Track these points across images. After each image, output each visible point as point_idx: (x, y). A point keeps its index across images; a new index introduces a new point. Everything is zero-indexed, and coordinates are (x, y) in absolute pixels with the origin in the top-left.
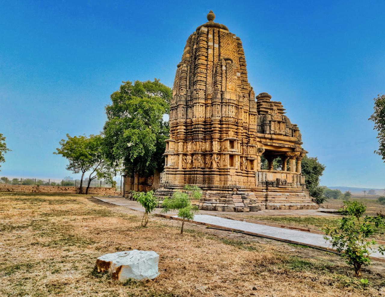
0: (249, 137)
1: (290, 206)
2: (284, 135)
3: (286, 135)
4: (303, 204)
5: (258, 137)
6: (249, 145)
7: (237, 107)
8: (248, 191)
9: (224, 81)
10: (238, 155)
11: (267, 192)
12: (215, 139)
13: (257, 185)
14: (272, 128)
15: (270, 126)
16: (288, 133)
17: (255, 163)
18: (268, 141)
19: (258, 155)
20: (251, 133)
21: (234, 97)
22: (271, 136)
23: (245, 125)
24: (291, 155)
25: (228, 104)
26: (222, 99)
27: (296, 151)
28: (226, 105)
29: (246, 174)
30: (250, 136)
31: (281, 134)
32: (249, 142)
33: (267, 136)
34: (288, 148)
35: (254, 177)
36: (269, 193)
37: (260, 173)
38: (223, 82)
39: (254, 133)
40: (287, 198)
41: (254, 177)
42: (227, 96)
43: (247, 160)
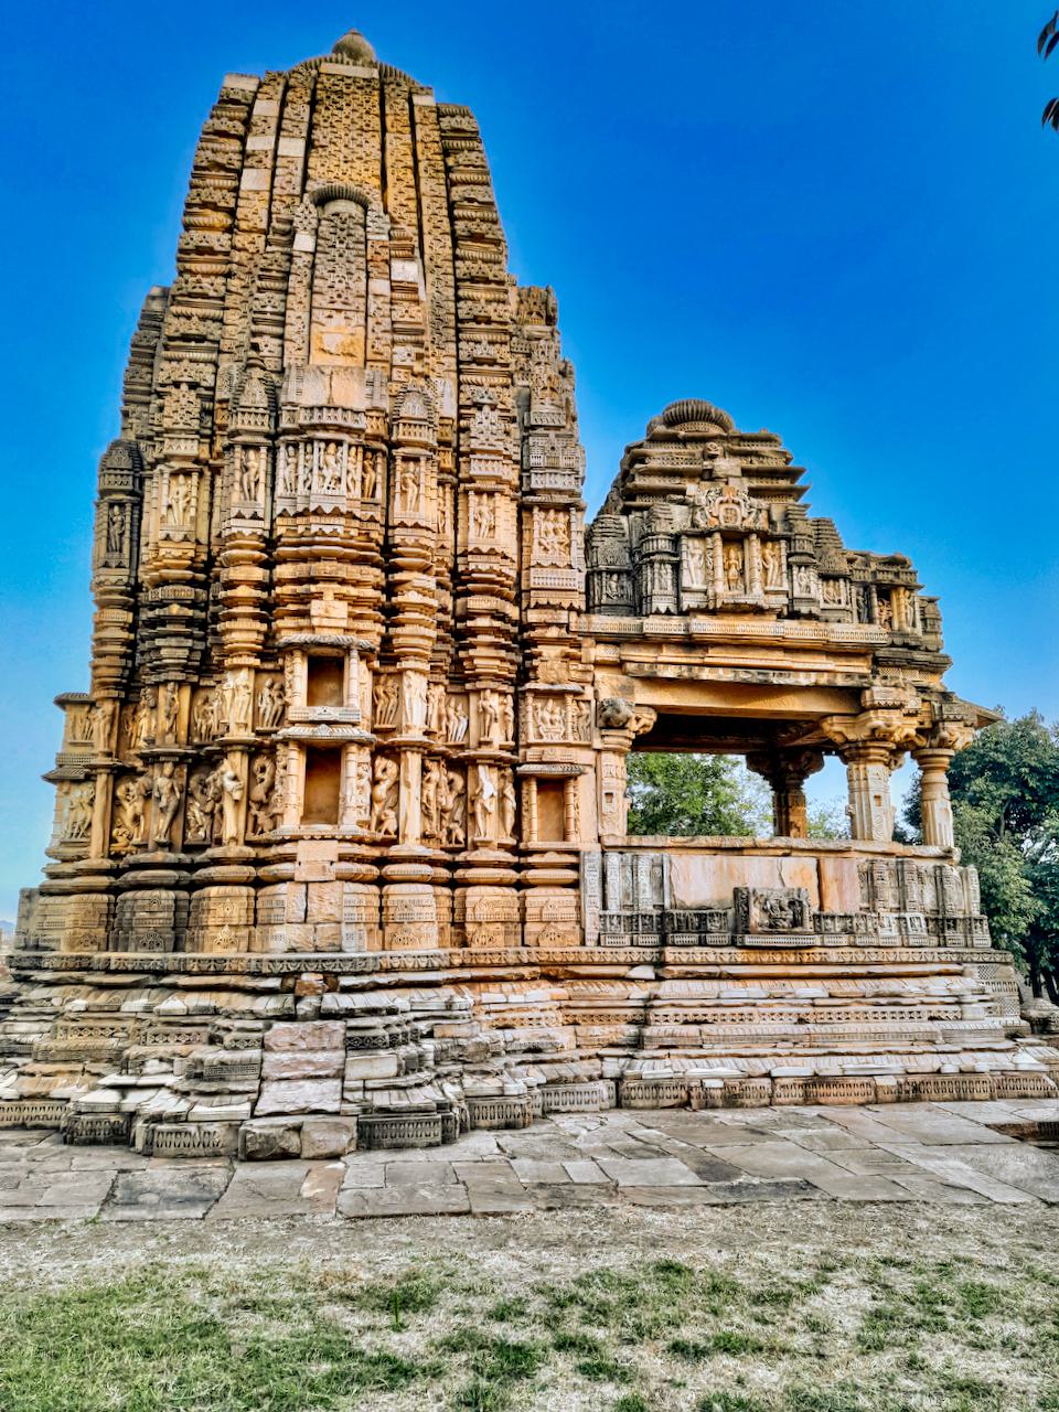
0: (534, 643)
1: (817, 1080)
2: (780, 616)
3: (794, 615)
4: (929, 1063)
5: (601, 639)
7: (383, 450)
8: (502, 979)
9: (296, 316)
10: (361, 744)
11: (659, 979)
12: (232, 653)
13: (591, 937)
14: (692, 577)
15: (677, 567)
16: (812, 601)
17: (581, 795)
18: (668, 654)
19: (597, 744)
21: (352, 394)
22: (687, 626)
23: (484, 567)
24: (851, 737)
25: (303, 437)
26: (275, 408)
27: (876, 708)
28: (296, 446)
29: (518, 867)
30: (537, 633)
31: (758, 611)
32: (524, 674)
33: (653, 625)
34: (816, 689)
35: (575, 885)
36: (667, 989)
37: (614, 859)
38: (291, 317)
39: (563, 617)
40: (801, 1021)
41: (575, 885)
42: (305, 393)
43: (519, 781)
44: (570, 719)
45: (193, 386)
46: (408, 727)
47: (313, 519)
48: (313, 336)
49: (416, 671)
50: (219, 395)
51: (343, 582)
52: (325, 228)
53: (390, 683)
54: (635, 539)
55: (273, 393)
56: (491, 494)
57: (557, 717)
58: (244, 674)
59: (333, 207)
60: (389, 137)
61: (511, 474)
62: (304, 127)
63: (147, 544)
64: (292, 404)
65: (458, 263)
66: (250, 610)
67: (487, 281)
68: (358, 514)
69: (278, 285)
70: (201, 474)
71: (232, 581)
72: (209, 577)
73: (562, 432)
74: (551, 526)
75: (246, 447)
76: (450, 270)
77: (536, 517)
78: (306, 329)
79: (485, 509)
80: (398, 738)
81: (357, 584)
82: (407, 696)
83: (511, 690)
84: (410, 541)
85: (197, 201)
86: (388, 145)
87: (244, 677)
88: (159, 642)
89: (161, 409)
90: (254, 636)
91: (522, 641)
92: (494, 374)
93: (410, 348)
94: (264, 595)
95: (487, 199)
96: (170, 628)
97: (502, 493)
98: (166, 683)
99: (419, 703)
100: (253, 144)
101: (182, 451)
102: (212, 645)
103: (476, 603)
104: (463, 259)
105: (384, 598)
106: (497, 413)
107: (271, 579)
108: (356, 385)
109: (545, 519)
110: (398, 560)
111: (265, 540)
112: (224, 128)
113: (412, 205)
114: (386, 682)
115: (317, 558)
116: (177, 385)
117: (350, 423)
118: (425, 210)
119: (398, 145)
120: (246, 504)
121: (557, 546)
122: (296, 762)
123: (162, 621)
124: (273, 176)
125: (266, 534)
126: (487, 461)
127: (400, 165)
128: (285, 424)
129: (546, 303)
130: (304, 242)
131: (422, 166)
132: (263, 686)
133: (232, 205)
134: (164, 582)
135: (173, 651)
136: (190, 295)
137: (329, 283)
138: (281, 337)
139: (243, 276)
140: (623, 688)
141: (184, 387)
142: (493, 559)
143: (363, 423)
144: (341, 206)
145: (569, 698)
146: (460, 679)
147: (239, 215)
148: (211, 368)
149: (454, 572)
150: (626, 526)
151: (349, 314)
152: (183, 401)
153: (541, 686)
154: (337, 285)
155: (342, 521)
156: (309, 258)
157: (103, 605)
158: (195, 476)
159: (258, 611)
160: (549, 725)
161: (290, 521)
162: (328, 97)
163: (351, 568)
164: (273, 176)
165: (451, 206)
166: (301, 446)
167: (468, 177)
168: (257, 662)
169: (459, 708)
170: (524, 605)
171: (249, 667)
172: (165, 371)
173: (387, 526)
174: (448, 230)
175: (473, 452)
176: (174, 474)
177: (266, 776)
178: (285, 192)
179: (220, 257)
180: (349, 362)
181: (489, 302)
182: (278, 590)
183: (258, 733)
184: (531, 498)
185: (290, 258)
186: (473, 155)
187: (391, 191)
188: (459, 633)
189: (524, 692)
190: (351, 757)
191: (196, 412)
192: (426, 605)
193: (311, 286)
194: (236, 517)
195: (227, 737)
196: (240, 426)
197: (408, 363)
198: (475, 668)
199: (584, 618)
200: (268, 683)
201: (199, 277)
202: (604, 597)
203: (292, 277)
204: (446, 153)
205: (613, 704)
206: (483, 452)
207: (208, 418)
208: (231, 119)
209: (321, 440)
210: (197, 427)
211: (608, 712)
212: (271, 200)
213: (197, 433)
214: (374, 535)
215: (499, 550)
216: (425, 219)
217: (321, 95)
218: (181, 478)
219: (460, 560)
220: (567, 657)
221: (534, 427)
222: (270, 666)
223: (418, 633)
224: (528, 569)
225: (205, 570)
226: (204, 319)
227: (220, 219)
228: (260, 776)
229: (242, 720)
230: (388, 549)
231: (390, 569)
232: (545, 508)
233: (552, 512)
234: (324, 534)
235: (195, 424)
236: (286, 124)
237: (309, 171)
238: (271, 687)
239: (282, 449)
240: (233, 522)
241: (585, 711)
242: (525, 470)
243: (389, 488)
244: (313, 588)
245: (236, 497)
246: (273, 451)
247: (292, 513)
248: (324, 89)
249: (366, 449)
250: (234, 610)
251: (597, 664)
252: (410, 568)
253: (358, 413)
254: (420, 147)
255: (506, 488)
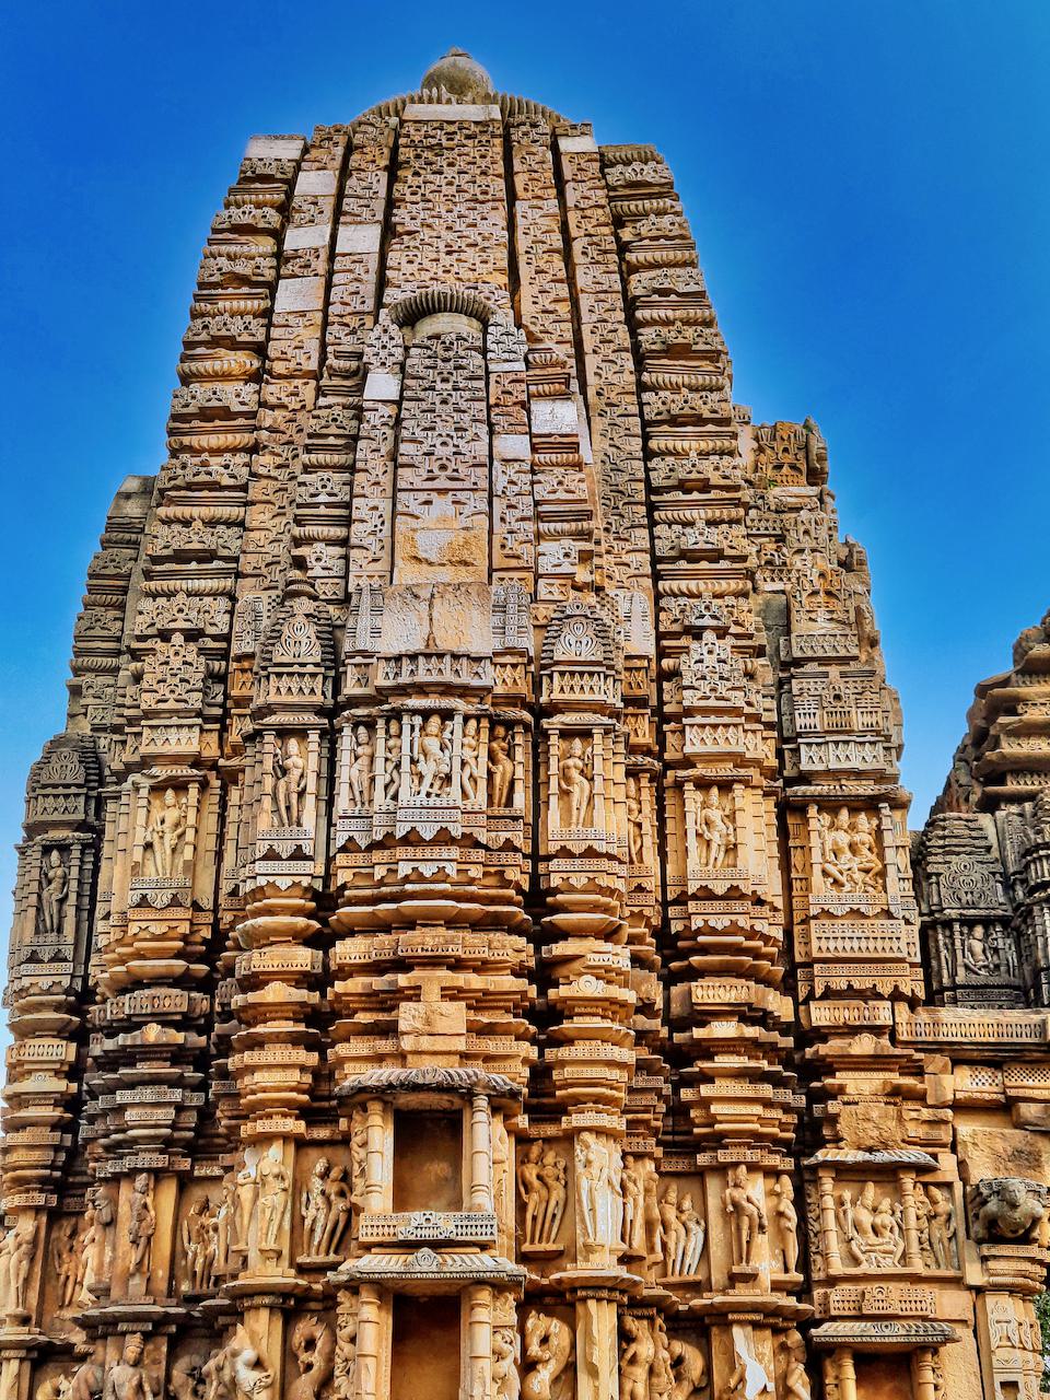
0: (826, 1067)
5: (960, 1056)
6: (826, 1154)
7: (525, 721)
9: (369, 506)
10: (499, 1287)
12: (256, 1110)
19: (975, 1275)
20: (846, 1013)
21: (471, 630)
25: (384, 709)
26: (334, 661)
28: (370, 725)
30: (832, 1047)
32: (812, 1132)
38: (361, 508)
39: (882, 1013)
42: (388, 632)
43: (818, 1358)
44: (913, 1223)
45: (192, 635)
46: (589, 1249)
47: (400, 852)
48: (398, 537)
49: (599, 1132)
50: (235, 650)
51: (457, 965)
52: (416, 360)
53: (550, 1158)
54: (1011, 857)
55: (331, 637)
56: (725, 786)
57: (886, 1219)
58: (275, 1151)
59: (428, 327)
60: (520, 207)
61: (761, 748)
62: (379, 206)
63: (107, 917)
64: (364, 653)
65: (646, 397)
66: (289, 1027)
67: (699, 420)
68: (483, 838)
69: (336, 459)
70: (204, 785)
71: (255, 975)
72: (214, 969)
73: (853, 667)
74: (843, 839)
75: (283, 733)
76: (635, 409)
77: (813, 824)
78: (388, 524)
79: (716, 815)
80: (570, 1272)
81: (483, 967)
82: (584, 1184)
83: (788, 1164)
84: (580, 881)
85: (204, 336)
86: (519, 221)
87: (275, 1157)
88: (122, 1097)
89: (137, 678)
90: (294, 1077)
91: (804, 1065)
92: (718, 576)
93: (567, 542)
94: (314, 998)
95: (693, 288)
96: (143, 1068)
97: (747, 783)
98: (132, 1174)
99: (608, 1200)
100: (295, 239)
101: (172, 748)
102: (218, 1096)
103: (707, 992)
104: (654, 388)
105: (533, 991)
106: (729, 641)
107: (326, 965)
108: (475, 613)
109: (832, 826)
110: (559, 918)
111: (315, 896)
112: (246, 220)
113: (564, 309)
114: (541, 1158)
115: (409, 923)
116: (165, 636)
117: (466, 679)
118: (585, 316)
119: (537, 218)
120: (284, 830)
121: (858, 876)
122: (372, 1326)
123: (128, 1056)
124: (329, 286)
125: (318, 885)
126: (715, 726)
127: (541, 248)
128: (351, 688)
129: (806, 448)
130: (382, 385)
131: (577, 247)
132: (310, 1171)
133: (261, 338)
134: (135, 983)
135: (147, 1111)
136: (189, 487)
137: (425, 448)
138: (344, 542)
139: (278, 450)
140: (1017, 1154)
141: (178, 639)
142: (737, 906)
143: (489, 676)
144: (443, 323)
145: (908, 1180)
146: (684, 1147)
147: (272, 353)
148: (224, 603)
149: (662, 935)
150: (991, 832)
151: (461, 496)
152: (176, 662)
153: (850, 1155)
154: (440, 451)
155: (455, 852)
156: (391, 410)
157: (23, 1031)
158: (193, 790)
159: (301, 1028)
160: (872, 1238)
161: (359, 859)
162: (418, 157)
163: (470, 937)
164: (329, 286)
165: (631, 304)
166: (381, 723)
167: (658, 256)
168: (299, 1127)
169: (687, 1204)
170: (802, 992)
171: (286, 1138)
172: (144, 614)
173: (535, 857)
174: (627, 344)
175: (689, 712)
176: (158, 789)
177: (316, 1358)
178: (349, 309)
179: (241, 421)
180: (463, 575)
181: (704, 455)
182: (339, 986)
183: (302, 1270)
184: (801, 789)
185: (359, 412)
186: (667, 219)
187: (526, 292)
188: (677, 1054)
189: (814, 1169)
190: (481, 1314)
191: (197, 679)
192: (613, 1001)
193: (394, 456)
194: (265, 858)
195: (243, 1280)
196: (273, 698)
197: (566, 569)
198: (712, 1120)
199: (923, 1015)
200: (320, 1167)
201: (205, 456)
202: (961, 971)
203: (361, 444)
204: (618, 222)
205: (1001, 1191)
206: (706, 711)
207: (219, 688)
208: (259, 206)
209: (414, 712)
210: (198, 705)
211: (993, 1206)
212: (326, 324)
213: (199, 714)
214: (512, 874)
215: (747, 889)
216: (586, 329)
217: (405, 154)
218: (170, 793)
219: (672, 911)
220: (896, 1094)
221: (798, 663)
222: (322, 1133)
223: (600, 1058)
224: (805, 921)
225: (208, 956)
226: (211, 523)
227: (243, 361)
228: (304, 1357)
229: (272, 1245)
230: (538, 898)
231: (544, 936)
232: (830, 805)
233: (844, 814)
234: (422, 879)
235: (195, 700)
236: (349, 204)
237: (389, 273)
238: (324, 1176)
239: (347, 731)
240: (260, 867)
241: (944, 1206)
242: (787, 740)
243: (538, 787)
244: (403, 980)
245: (265, 821)
246: (330, 736)
247: (363, 844)
248: (412, 145)
249: (495, 722)
250: (260, 1029)
251: (962, 1107)
252: (580, 932)
253: (478, 660)
254: (573, 217)
255: (753, 772)
